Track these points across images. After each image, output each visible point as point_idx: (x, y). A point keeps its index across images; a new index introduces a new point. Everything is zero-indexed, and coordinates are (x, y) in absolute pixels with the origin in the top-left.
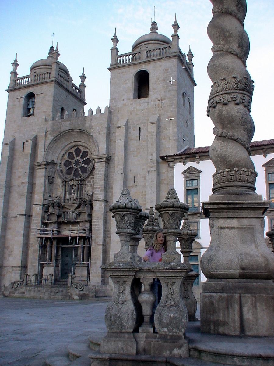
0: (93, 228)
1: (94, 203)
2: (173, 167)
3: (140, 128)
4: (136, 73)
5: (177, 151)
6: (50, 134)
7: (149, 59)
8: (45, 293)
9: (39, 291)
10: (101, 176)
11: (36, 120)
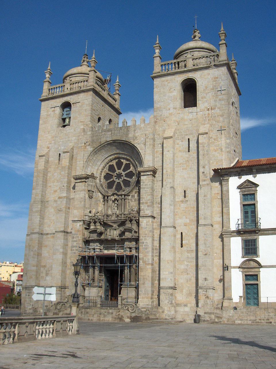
0: (141, 246)
1: (141, 219)
2: (227, 180)
3: (189, 139)
4: (182, 81)
5: (231, 164)
6: (89, 145)
7: (196, 67)
8: (93, 315)
9: (87, 313)
10: (147, 190)
11: (72, 131)
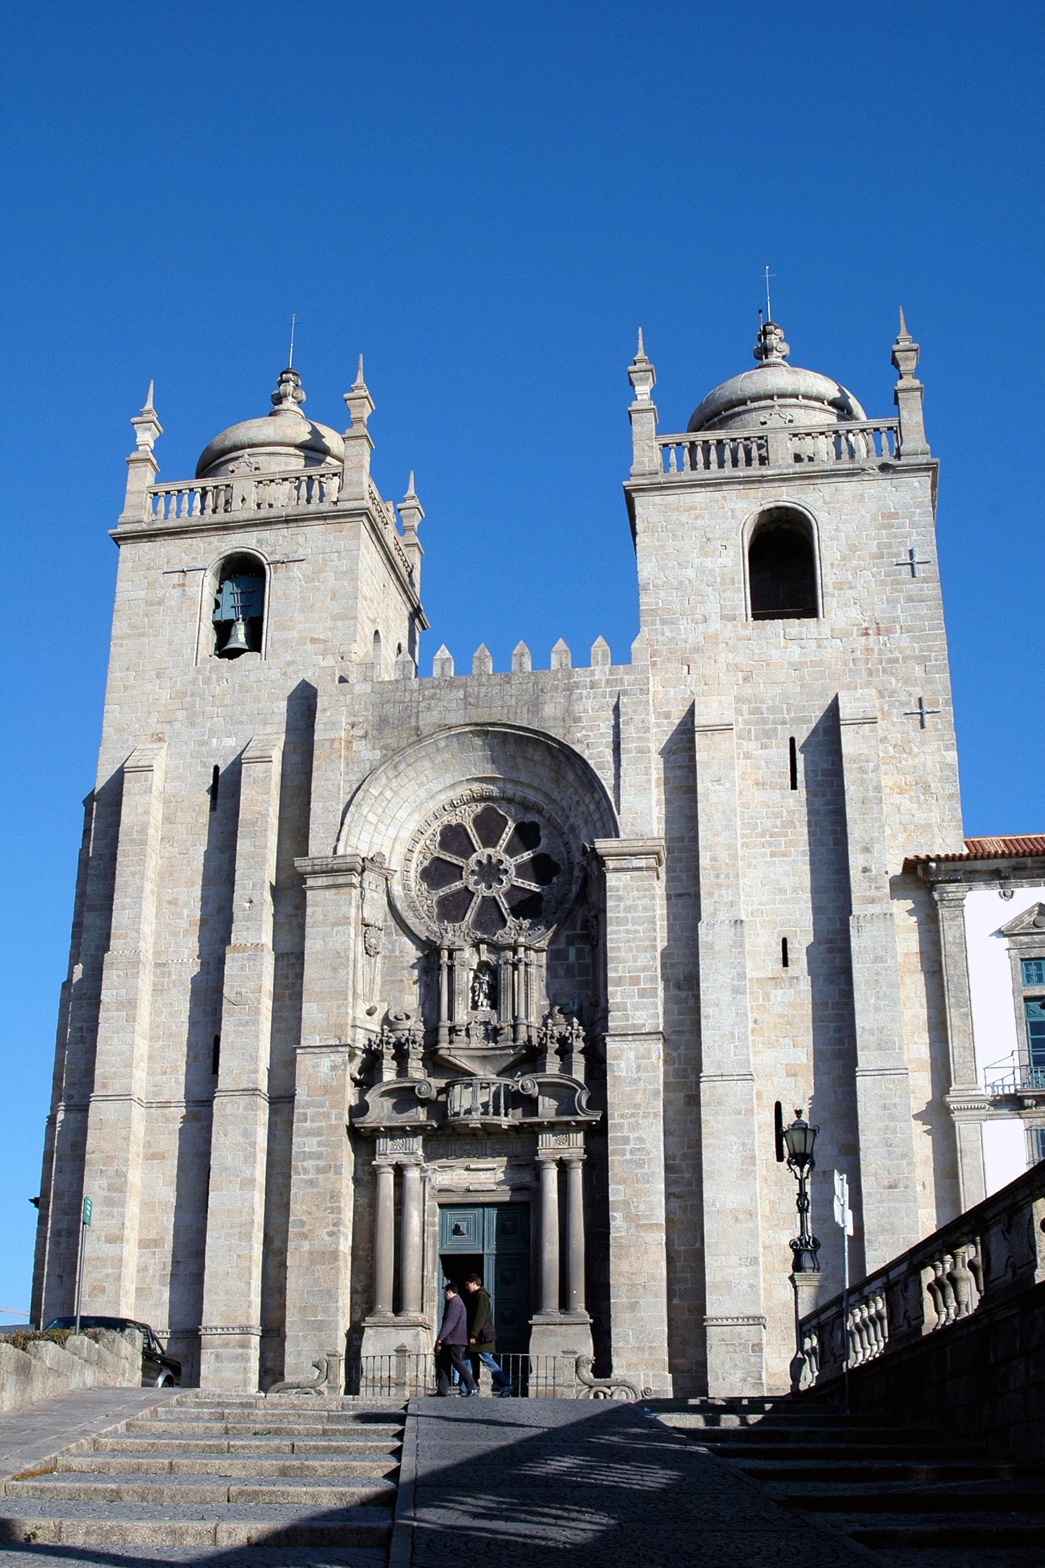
2: (959, 904)
6: (365, 737)
10: (637, 927)
